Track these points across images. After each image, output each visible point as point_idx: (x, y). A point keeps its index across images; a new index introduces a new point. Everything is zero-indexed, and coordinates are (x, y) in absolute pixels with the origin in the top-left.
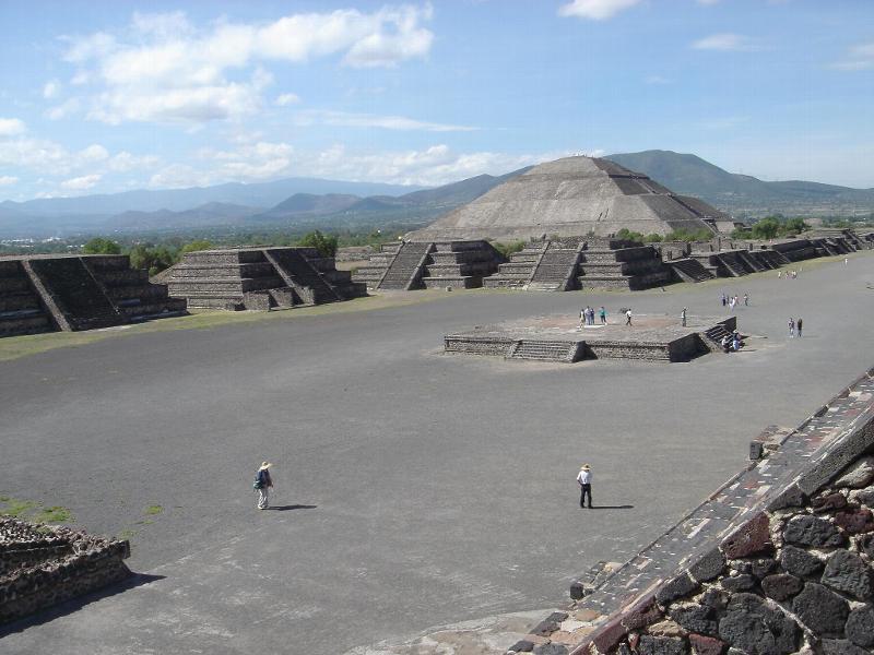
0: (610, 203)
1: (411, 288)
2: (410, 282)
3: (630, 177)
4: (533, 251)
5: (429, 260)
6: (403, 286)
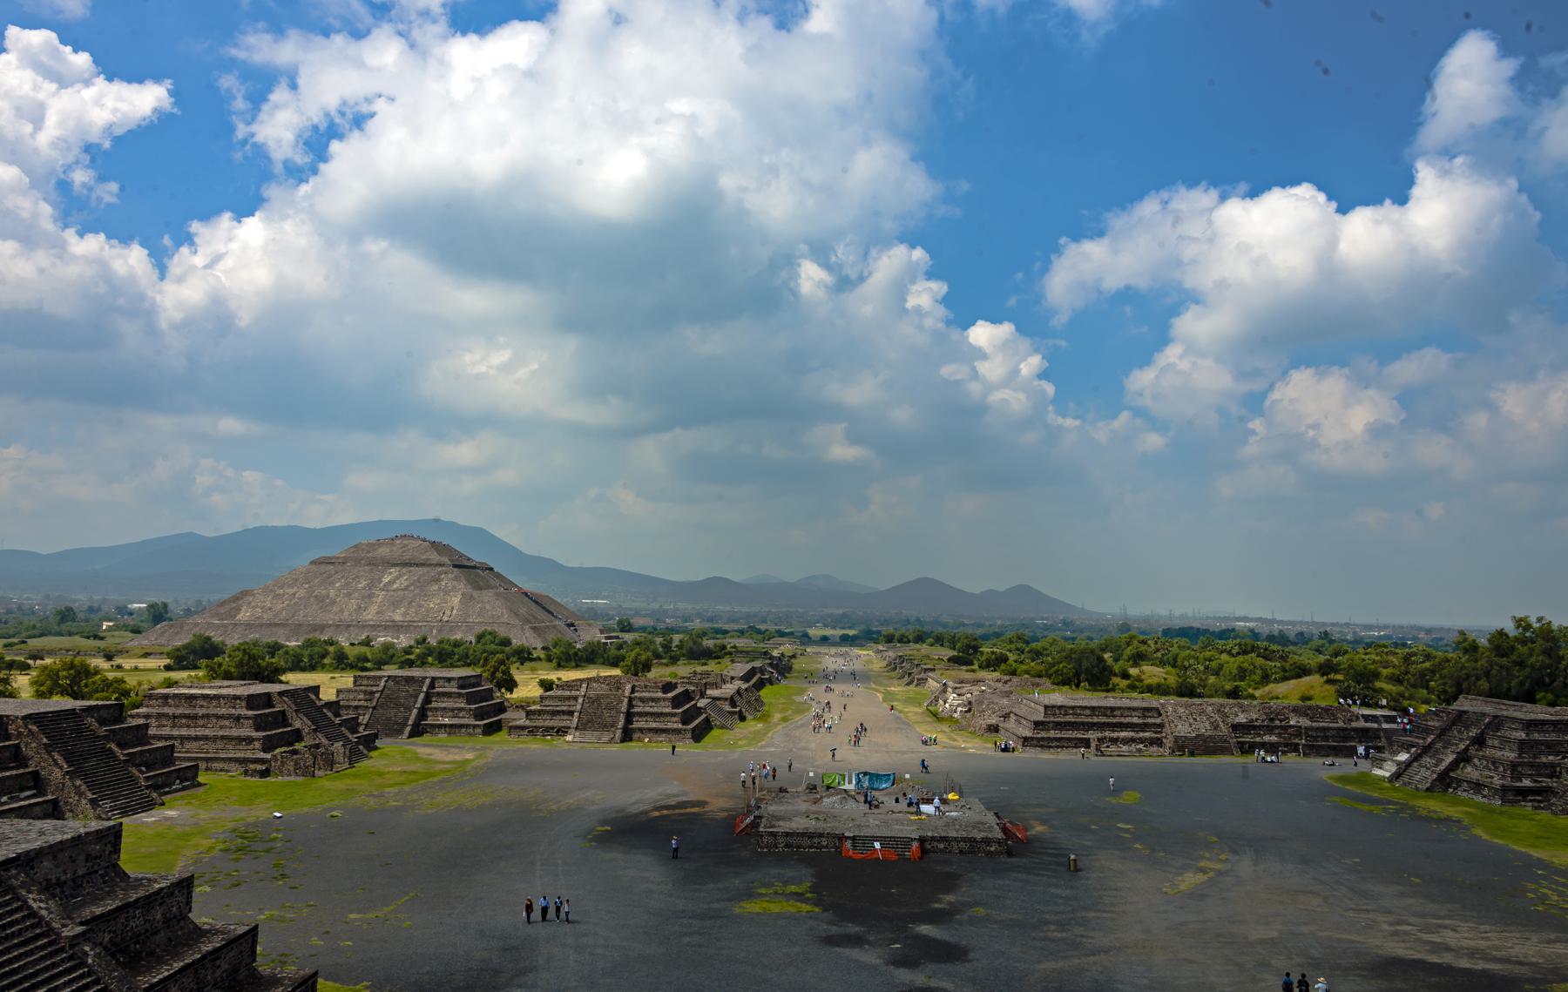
0: (456, 600)
3: (474, 567)
5: (428, 700)
6: (400, 732)
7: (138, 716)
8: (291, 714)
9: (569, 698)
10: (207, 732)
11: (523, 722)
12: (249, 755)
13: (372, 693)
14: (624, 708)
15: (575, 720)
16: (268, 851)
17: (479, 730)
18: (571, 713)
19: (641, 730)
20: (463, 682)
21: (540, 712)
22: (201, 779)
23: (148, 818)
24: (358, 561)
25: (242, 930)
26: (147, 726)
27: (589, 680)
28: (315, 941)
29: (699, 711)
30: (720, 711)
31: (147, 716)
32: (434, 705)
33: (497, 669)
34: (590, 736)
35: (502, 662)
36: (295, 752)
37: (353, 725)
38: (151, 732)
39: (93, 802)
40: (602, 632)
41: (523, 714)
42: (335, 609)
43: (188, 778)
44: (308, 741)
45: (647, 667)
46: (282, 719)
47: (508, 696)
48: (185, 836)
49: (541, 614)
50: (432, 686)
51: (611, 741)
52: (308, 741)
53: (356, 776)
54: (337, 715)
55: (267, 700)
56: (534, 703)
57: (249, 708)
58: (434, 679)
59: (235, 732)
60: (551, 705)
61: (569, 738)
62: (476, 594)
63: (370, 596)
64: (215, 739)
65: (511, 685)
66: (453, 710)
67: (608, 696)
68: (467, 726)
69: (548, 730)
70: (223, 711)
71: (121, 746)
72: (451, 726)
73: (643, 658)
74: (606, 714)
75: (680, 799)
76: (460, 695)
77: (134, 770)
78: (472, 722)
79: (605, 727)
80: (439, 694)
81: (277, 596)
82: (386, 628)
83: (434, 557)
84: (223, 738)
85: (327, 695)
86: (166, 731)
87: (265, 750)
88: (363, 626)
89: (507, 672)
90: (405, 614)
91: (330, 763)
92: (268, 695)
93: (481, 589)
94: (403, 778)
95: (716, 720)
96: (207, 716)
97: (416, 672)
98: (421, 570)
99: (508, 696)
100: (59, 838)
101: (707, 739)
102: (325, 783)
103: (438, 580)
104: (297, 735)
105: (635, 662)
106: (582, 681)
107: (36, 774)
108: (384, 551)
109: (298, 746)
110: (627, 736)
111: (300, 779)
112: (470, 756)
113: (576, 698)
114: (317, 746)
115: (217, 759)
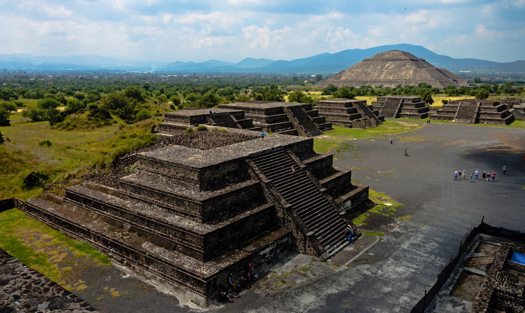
0: (411, 72)
1: (396, 117)
2: (395, 115)
4: (453, 105)
5: (401, 106)
6: (392, 116)
7: (315, 108)
8: (358, 109)
9: (454, 107)
10: (334, 114)
11: (436, 114)
12: (346, 121)
13: (383, 103)
14: (476, 111)
15: (456, 115)
16: (353, 150)
17: (420, 117)
18: (455, 112)
19: (483, 119)
20: (414, 100)
21: (442, 112)
22: (333, 127)
23: (320, 137)
24: (378, 60)
25: (347, 172)
26: (318, 111)
27: (462, 101)
28: (368, 178)
29: (509, 113)
30: (519, 113)
31: (318, 108)
32: (404, 108)
33: (426, 96)
34: (462, 121)
35: (428, 94)
36: (359, 121)
37: (377, 113)
38: (319, 113)
39: (305, 132)
40: (467, 83)
41: (436, 112)
42: (371, 76)
43: (329, 127)
44: (363, 118)
45: (487, 96)
46: (355, 110)
47: (430, 105)
48: (329, 143)
49: (443, 77)
50: (403, 101)
51: (471, 123)
52: (363, 118)
53: (378, 129)
54: (372, 110)
55: (350, 105)
56: (440, 108)
57: (346, 107)
58: (404, 99)
59: (342, 114)
60: (447, 109)
61: (454, 121)
62: (419, 70)
63: (382, 71)
64: (336, 116)
65: (431, 102)
66: (410, 110)
67: (470, 107)
68: (415, 115)
69: (445, 118)
70: (338, 107)
71: (312, 117)
72: (410, 115)
73: (485, 93)
74: (469, 113)
75: (499, 145)
76: (413, 105)
77: (315, 123)
78: (417, 114)
79: (468, 118)
80: (405, 104)
81: (352, 72)
82: (387, 82)
83: (404, 57)
84: (338, 115)
85: (369, 103)
86: (323, 113)
87: (351, 120)
88: (380, 82)
89: (430, 97)
90: (393, 77)
91: (370, 125)
92: (351, 103)
93: (420, 68)
94: (393, 131)
95: (516, 116)
96: (334, 109)
97: (397, 97)
98: (399, 62)
99: (430, 105)
100: (298, 141)
101: (512, 124)
102: (369, 131)
103: (405, 65)
104: (360, 116)
105: (481, 94)
106: (459, 101)
107: (291, 123)
108: (386, 56)
109: (360, 119)
110: (477, 121)
111: (361, 129)
112: (416, 125)
113: (457, 107)
114: (366, 119)
115: (337, 122)
